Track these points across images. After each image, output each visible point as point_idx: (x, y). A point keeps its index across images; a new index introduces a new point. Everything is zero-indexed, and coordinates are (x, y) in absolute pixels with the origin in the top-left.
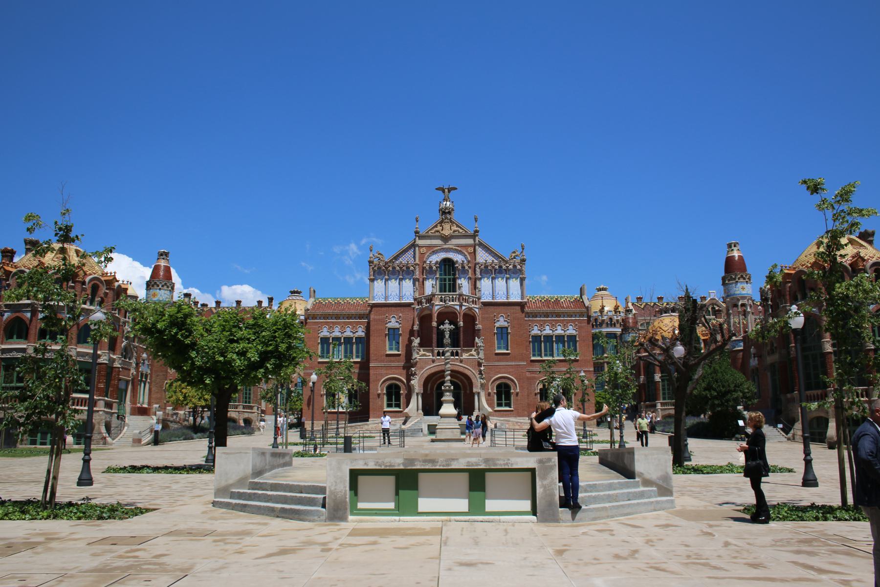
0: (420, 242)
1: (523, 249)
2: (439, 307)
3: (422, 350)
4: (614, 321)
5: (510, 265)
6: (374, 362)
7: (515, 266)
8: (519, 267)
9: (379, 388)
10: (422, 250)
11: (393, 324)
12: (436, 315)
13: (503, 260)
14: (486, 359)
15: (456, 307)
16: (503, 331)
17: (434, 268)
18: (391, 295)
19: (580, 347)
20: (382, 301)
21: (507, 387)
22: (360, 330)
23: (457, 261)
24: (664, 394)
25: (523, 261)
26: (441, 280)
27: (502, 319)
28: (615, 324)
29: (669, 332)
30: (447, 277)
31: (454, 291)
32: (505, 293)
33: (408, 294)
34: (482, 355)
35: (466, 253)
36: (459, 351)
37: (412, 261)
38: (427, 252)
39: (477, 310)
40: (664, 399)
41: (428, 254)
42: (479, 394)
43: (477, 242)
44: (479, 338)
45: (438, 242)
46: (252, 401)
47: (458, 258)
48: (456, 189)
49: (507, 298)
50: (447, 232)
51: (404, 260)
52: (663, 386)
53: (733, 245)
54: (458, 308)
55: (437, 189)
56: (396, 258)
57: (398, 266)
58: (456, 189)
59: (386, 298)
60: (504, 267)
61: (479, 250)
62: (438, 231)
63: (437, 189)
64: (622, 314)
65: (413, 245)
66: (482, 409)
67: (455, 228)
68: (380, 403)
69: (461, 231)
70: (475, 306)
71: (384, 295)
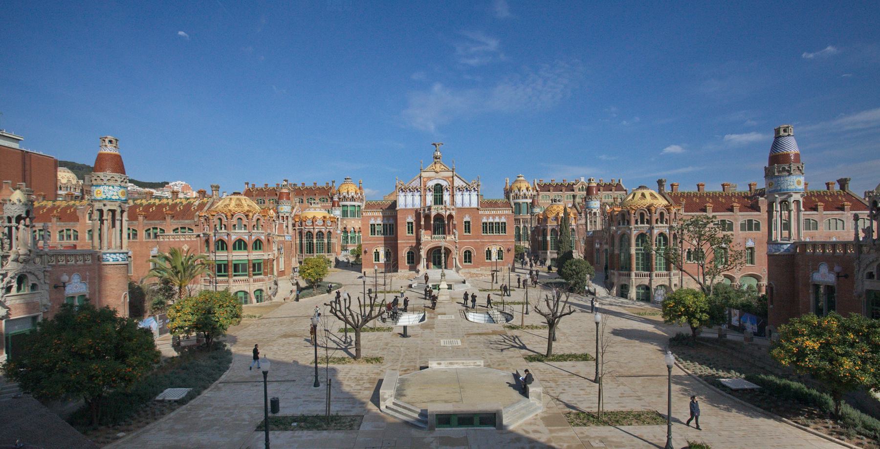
9: (403, 253)
14: (459, 238)
16: (468, 223)
21: (469, 252)
26: (435, 196)
27: (467, 216)
30: (438, 194)
31: (442, 204)
45: (433, 174)
47: (444, 183)
67: (443, 167)
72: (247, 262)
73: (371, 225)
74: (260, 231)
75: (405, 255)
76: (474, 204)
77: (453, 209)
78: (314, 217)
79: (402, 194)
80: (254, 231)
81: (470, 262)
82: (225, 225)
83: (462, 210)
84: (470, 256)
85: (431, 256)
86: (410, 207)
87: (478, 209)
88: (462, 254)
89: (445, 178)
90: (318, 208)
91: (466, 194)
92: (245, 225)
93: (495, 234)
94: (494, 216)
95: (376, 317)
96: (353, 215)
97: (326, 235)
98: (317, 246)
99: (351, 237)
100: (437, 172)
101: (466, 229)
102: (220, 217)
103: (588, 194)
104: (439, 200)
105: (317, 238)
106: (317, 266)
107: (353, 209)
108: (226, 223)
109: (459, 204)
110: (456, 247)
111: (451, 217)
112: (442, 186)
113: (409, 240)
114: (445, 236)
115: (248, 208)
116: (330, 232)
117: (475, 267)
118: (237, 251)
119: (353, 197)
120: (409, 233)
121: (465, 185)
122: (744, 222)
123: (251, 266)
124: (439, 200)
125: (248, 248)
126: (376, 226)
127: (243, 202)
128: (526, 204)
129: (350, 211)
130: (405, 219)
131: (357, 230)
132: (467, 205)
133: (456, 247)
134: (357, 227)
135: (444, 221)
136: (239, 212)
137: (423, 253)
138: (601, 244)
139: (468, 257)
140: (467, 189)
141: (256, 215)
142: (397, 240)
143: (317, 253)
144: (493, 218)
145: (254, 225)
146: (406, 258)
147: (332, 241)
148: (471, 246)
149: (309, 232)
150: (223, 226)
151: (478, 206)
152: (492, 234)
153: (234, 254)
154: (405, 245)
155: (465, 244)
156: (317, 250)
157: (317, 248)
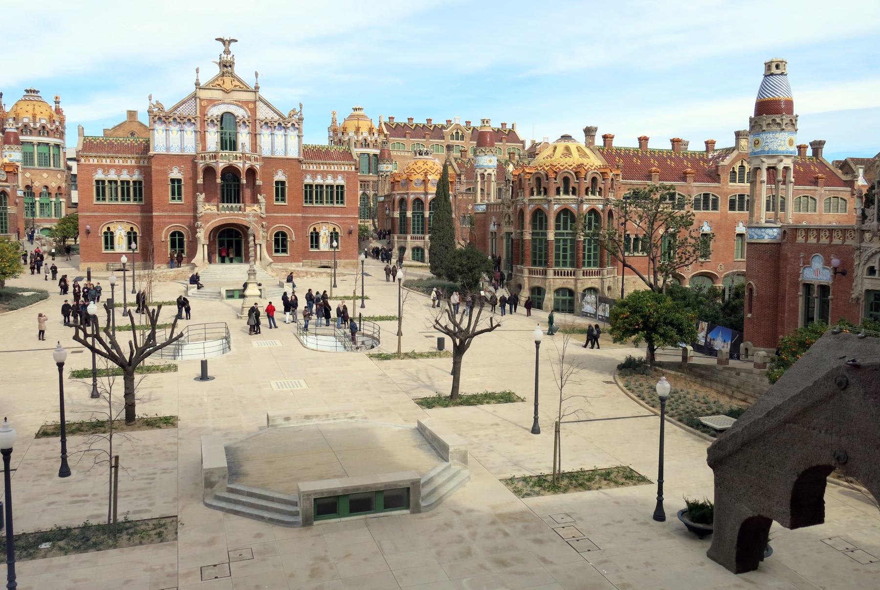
0: (203, 94)
1: (301, 108)
2: (223, 164)
3: (207, 205)
4: (368, 141)
5: (289, 122)
6: (157, 212)
7: (293, 125)
8: (297, 126)
9: (163, 236)
10: (202, 103)
11: (175, 174)
12: (220, 172)
13: (282, 118)
14: (267, 211)
15: (239, 164)
17: (216, 122)
18: (172, 146)
19: (347, 194)
20: (164, 152)
21: (284, 234)
22: (137, 172)
23: (238, 116)
24: (414, 228)
25: (301, 119)
27: (280, 173)
28: (368, 145)
29: (422, 175)
31: (235, 149)
32: (284, 149)
33: (189, 146)
34: (263, 210)
35: (247, 109)
36: (243, 207)
37: (193, 114)
38: (208, 105)
39: (258, 167)
40: (414, 233)
41: (209, 107)
42: (260, 245)
43: (258, 98)
44: (261, 195)
45: (217, 94)
46: (8, 230)
47: (240, 112)
48: (236, 41)
49: (286, 154)
50: (228, 86)
51: (184, 111)
52: (414, 221)
53: (485, 121)
54: (241, 165)
55: (216, 39)
56: (176, 108)
57: (179, 117)
58: (236, 41)
59: (168, 149)
60: (283, 125)
61: (260, 104)
62: (218, 85)
63: (216, 39)
64: (376, 135)
65: (194, 96)
66: (264, 259)
67: (236, 83)
68: (164, 250)
69: (242, 86)
70: (257, 163)
71: (165, 145)
73: (98, 182)
75: (166, 237)
76: (293, 153)
77: (256, 160)
79: (159, 128)
81: (284, 251)
83: (271, 162)
84: (284, 240)
85: (214, 240)
86: (175, 151)
87: (300, 161)
88: (271, 237)
89: (242, 104)
91: (279, 133)
93: (325, 205)
94: (324, 174)
95: (163, 346)
96: (45, 160)
99: (42, 205)
100: (226, 92)
101: (277, 195)
103: (479, 145)
104: (229, 143)
107: (44, 149)
109: (266, 152)
110: (262, 226)
111: (251, 172)
112: (235, 117)
113: (174, 211)
114: (242, 205)
117: (293, 259)
119: (44, 127)
120: (173, 198)
121: (276, 117)
122: (699, 197)
124: (229, 143)
126: (107, 183)
128: (366, 156)
129: (39, 154)
130: (166, 174)
132: (279, 154)
133: (262, 226)
134: (53, 185)
135: (239, 180)
137: (202, 235)
138: (499, 225)
139: (280, 242)
140: (280, 124)
142: (152, 212)
144: (324, 177)
146: (169, 243)
147: (9, 211)
148: (286, 224)
151: (299, 155)
152: (331, 205)
154: (167, 220)
155: (276, 220)
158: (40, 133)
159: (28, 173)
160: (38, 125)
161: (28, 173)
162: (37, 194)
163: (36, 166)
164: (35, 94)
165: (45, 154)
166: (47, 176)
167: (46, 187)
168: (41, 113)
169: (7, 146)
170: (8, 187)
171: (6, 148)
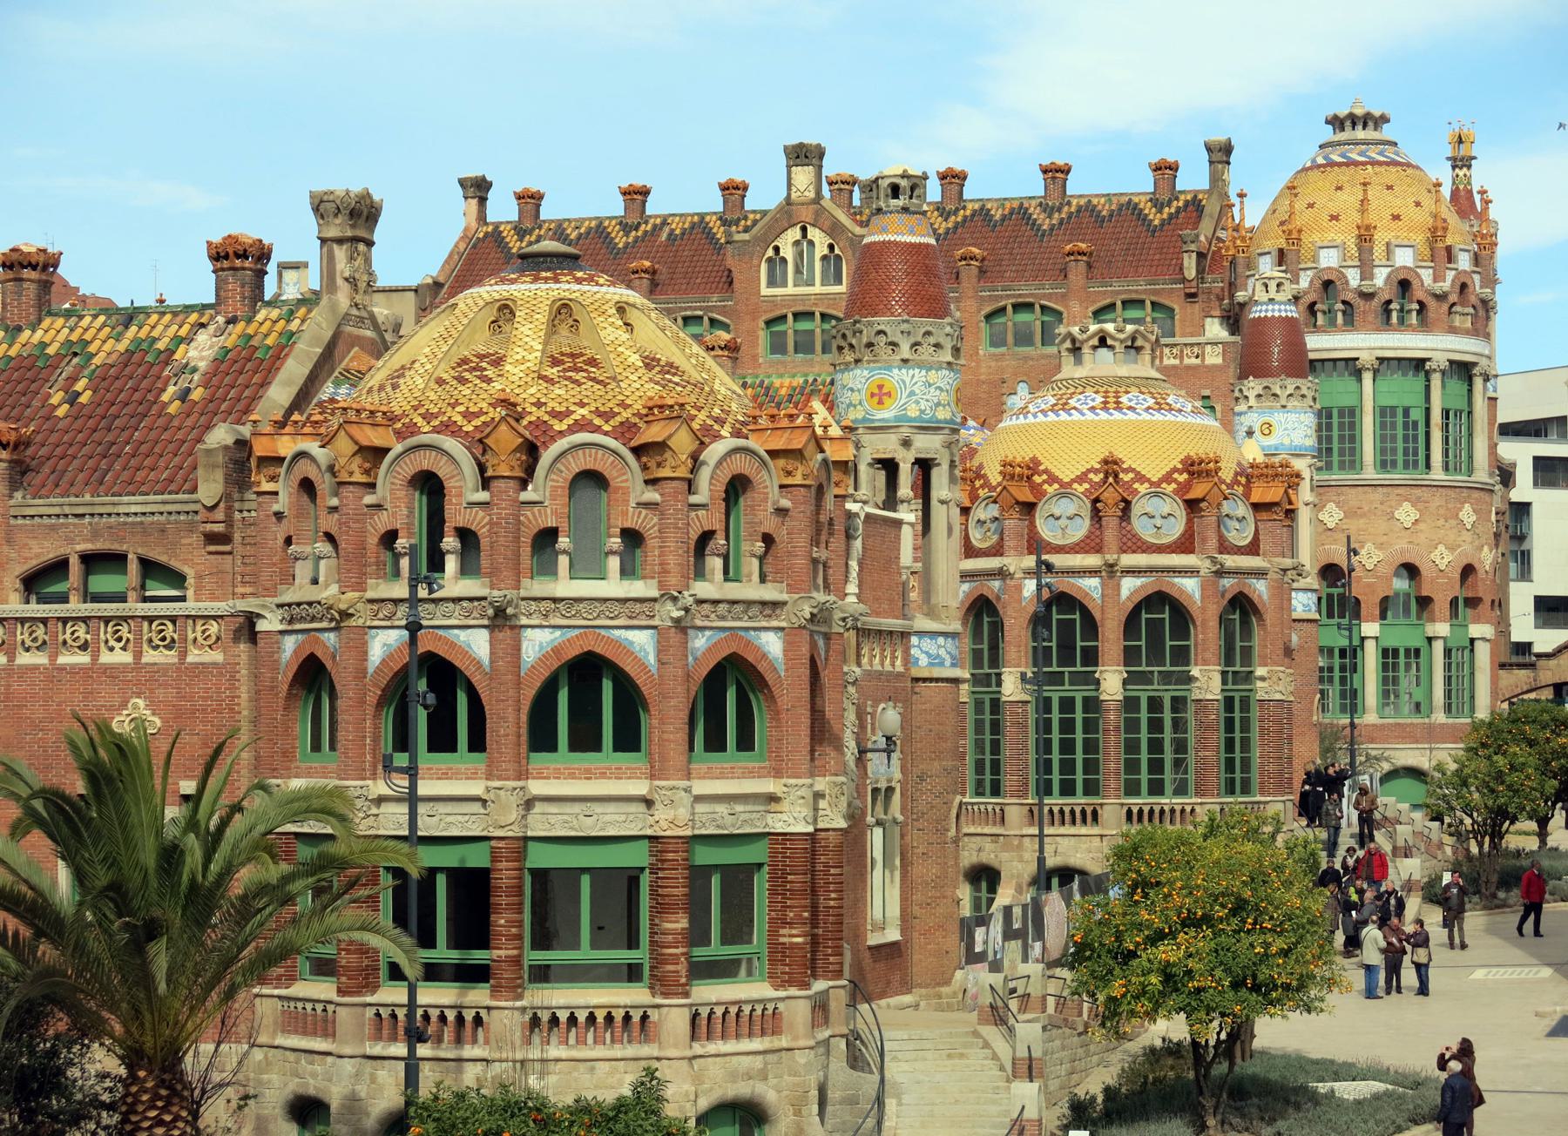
72: (636, 856)
74: (752, 590)
78: (1111, 467)
80: (703, 589)
82: (467, 537)
90: (1142, 383)
92: (633, 538)
97: (1206, 634)
98: (1132, 726)
102: (425, 461)
105: (1130, 656)
106: (1239, 907)
108: (477, 521)
115: (652, 390)
116: (1242, 607)
118: (563, 755)
123: (677, 890)
125: (649, 724)
127: (611, 331)
131: (1442, 590)
134: (1441, 560)
136: (580, 426)
141: (715, 451)
143: (1132, 789)
145: (706, 537)
147: (1262, 690)
149: (1064, 601)
150: (450, 542)
153: (537, 787)
156: (1132, 766)
157: (1132, 747)
158: (1388, 312)
159: (1331, 506)
160: (1380, 277)
161: (1331, 506)
162: (1370, 605)
163: (1370, 473)
164: (1369, 134)
165: (1406, 412)
166: (1415, 515)
167: (1411, 570)
168: (1396, 217)
169: (1253, 386)
170: (1260, 574)
171: (1252, 395)
